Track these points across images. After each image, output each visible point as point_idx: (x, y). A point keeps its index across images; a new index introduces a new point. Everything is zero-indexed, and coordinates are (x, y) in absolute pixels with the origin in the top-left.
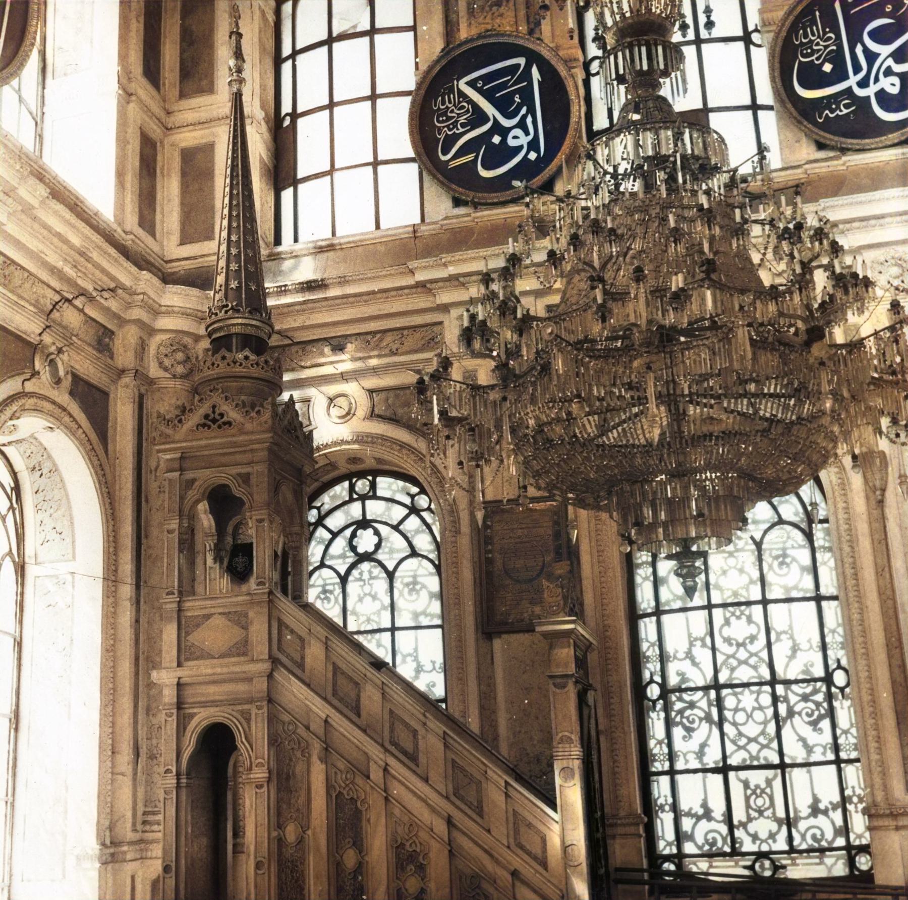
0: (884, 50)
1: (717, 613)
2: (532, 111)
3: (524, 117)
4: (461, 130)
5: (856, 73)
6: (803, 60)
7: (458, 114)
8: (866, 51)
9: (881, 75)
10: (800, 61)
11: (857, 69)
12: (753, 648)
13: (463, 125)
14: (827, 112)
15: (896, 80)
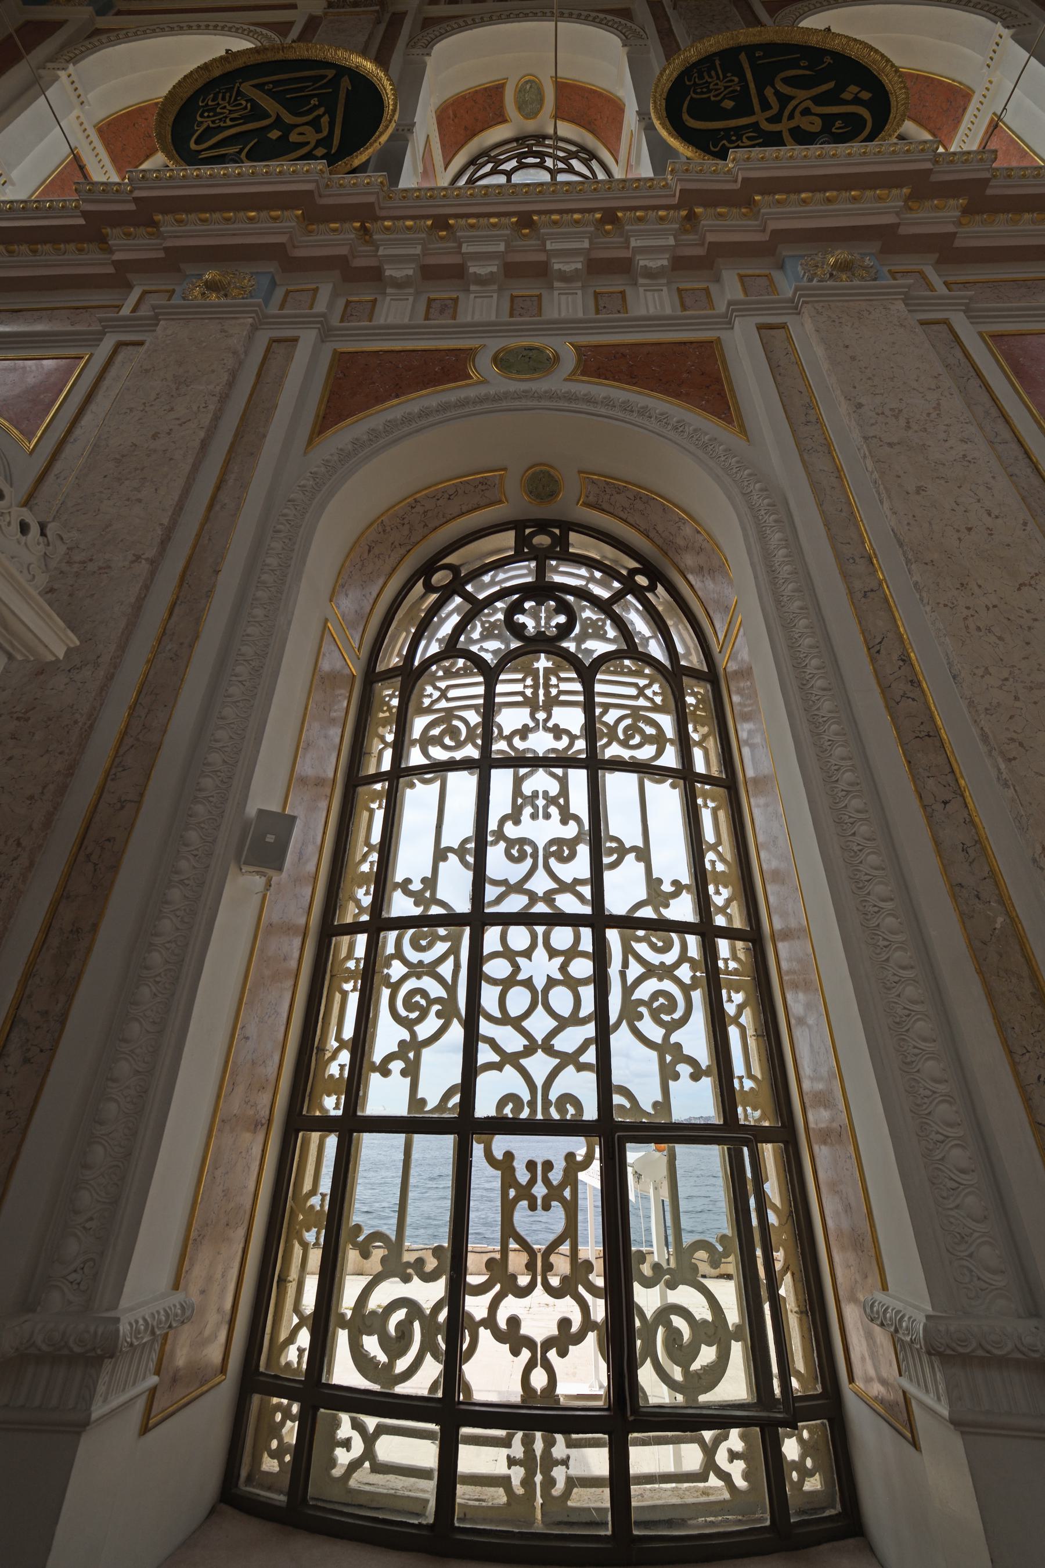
0: (801, 96)
1: (501, 780)
2: (331, 112)
3: (319, 117)
4: (229, 123)
5: (763, 110)
6: (695, 96)
7: (230, 111)
8: (777, 93)
9: (797, 113)
10: (691, 97)
11: (765, 106)
12: (567, 872)
13: (232, 120)
14: (724, 142)
15: (818, 121)
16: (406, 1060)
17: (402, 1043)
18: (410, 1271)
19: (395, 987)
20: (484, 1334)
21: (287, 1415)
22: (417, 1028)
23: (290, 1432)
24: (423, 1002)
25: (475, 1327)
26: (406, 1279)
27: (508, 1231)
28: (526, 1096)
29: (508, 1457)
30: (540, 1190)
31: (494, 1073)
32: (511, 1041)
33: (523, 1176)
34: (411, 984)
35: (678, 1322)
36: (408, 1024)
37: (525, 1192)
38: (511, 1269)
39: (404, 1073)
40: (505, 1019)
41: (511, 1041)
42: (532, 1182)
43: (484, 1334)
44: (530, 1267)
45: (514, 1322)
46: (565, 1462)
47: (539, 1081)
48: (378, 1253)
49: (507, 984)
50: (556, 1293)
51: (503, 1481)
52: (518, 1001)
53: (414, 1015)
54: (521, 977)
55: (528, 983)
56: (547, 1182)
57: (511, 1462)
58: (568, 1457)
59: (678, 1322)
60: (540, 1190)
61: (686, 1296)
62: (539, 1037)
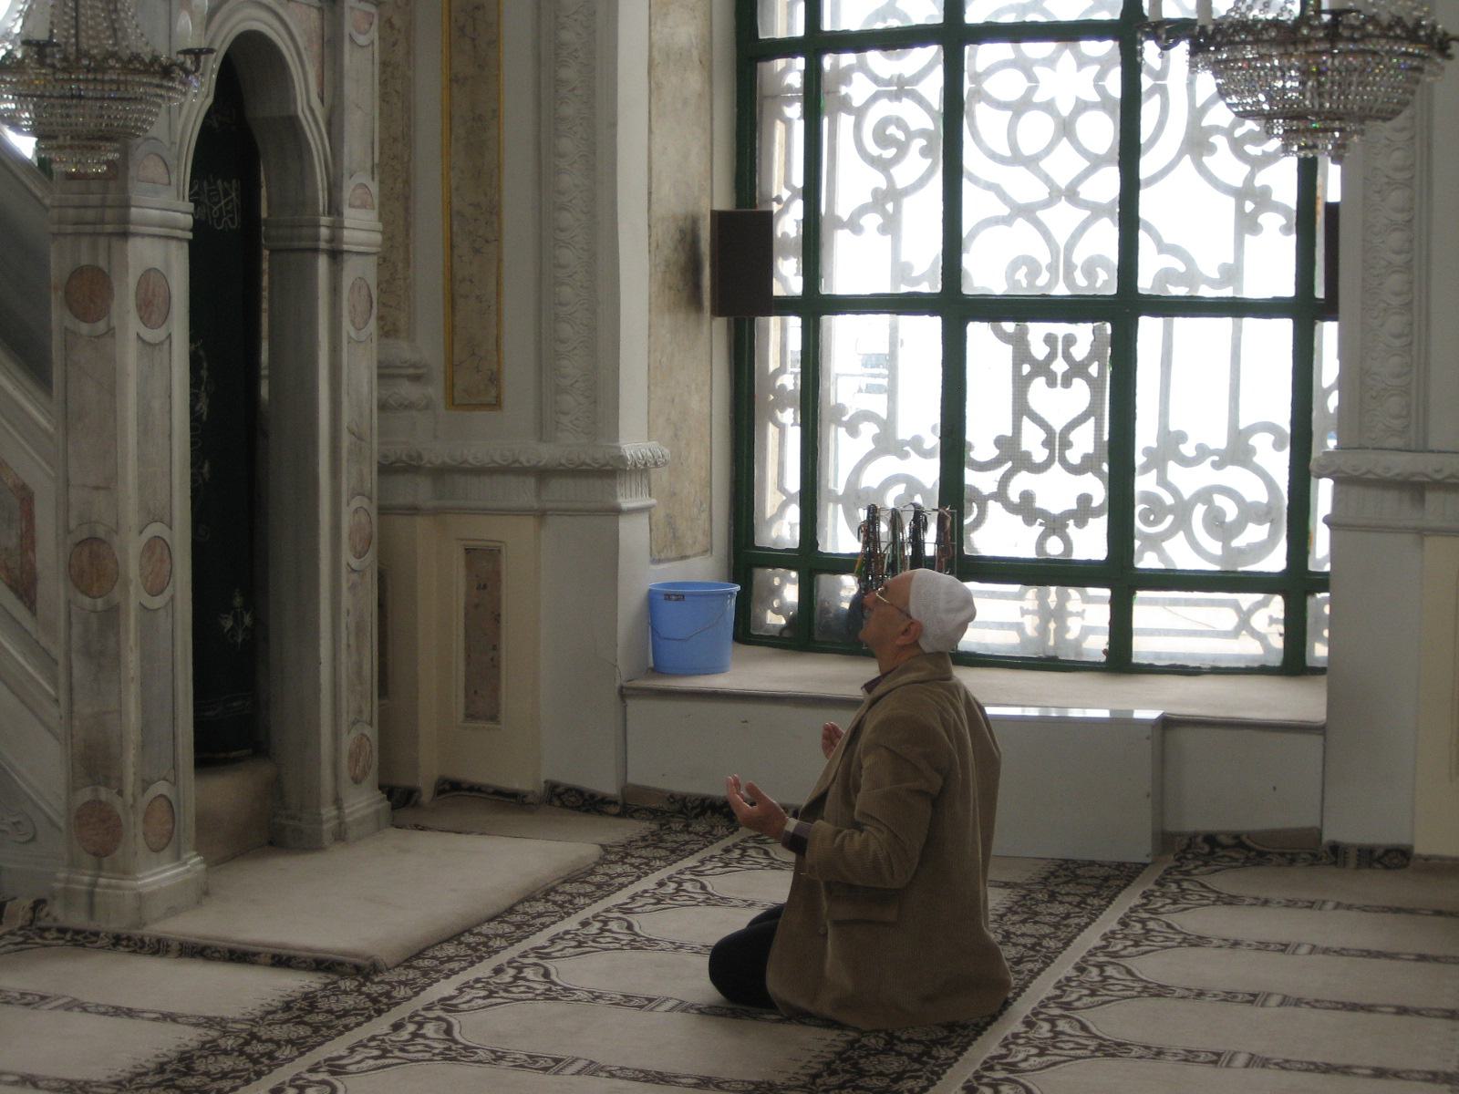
16: (884, 213)
17: (876, 192)
18: (907, 448)
19: (860, 113)
20: (994, 508)
21: (785, 580)
22: (894, 171)
23: (791, 594)
24: (901, 135)
25: (983, 501)
26: (904, 456)
27: (1021, 408)
28: (1044, 258)
29: (1021, 608)
30: (1059, 366)
31: (1002, 228)
32: (1026, 187)
33: (1039, 350)
34: (883, 108)
35: (1220, 500)
36: (882, 165)
37: (1042, 368)
38: (1025, 446)
39: (883, 230)
40: (1016, 158)
41: (1026, 187)
42: (1051, 357)
43: (994, 508)
44: (1048, 443)
45: (1027, 497)
46: (1081, 614)
47: (1061, 239)
48: (869, 430)
49: (1020, 107)
50: (1076, 470)
51: (1019, 627)
52: (1035, 131)
53: (889, 153)
54: (1037, 98)
55: (1049, 107)
56: (1067, 357)
57: (1024, 612)
58: (1084, 611)
59: (1220, 500)
60: (1059, 366)
61: (1234, 476)
62: (1063, 183)
